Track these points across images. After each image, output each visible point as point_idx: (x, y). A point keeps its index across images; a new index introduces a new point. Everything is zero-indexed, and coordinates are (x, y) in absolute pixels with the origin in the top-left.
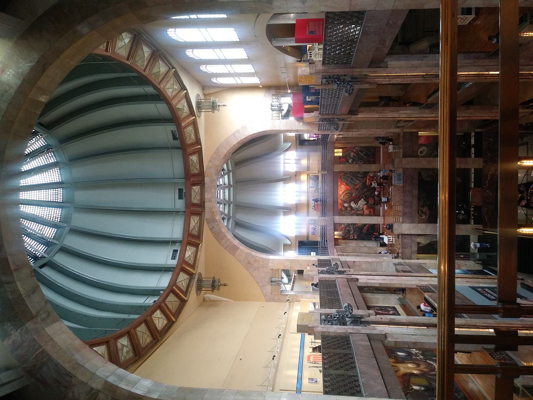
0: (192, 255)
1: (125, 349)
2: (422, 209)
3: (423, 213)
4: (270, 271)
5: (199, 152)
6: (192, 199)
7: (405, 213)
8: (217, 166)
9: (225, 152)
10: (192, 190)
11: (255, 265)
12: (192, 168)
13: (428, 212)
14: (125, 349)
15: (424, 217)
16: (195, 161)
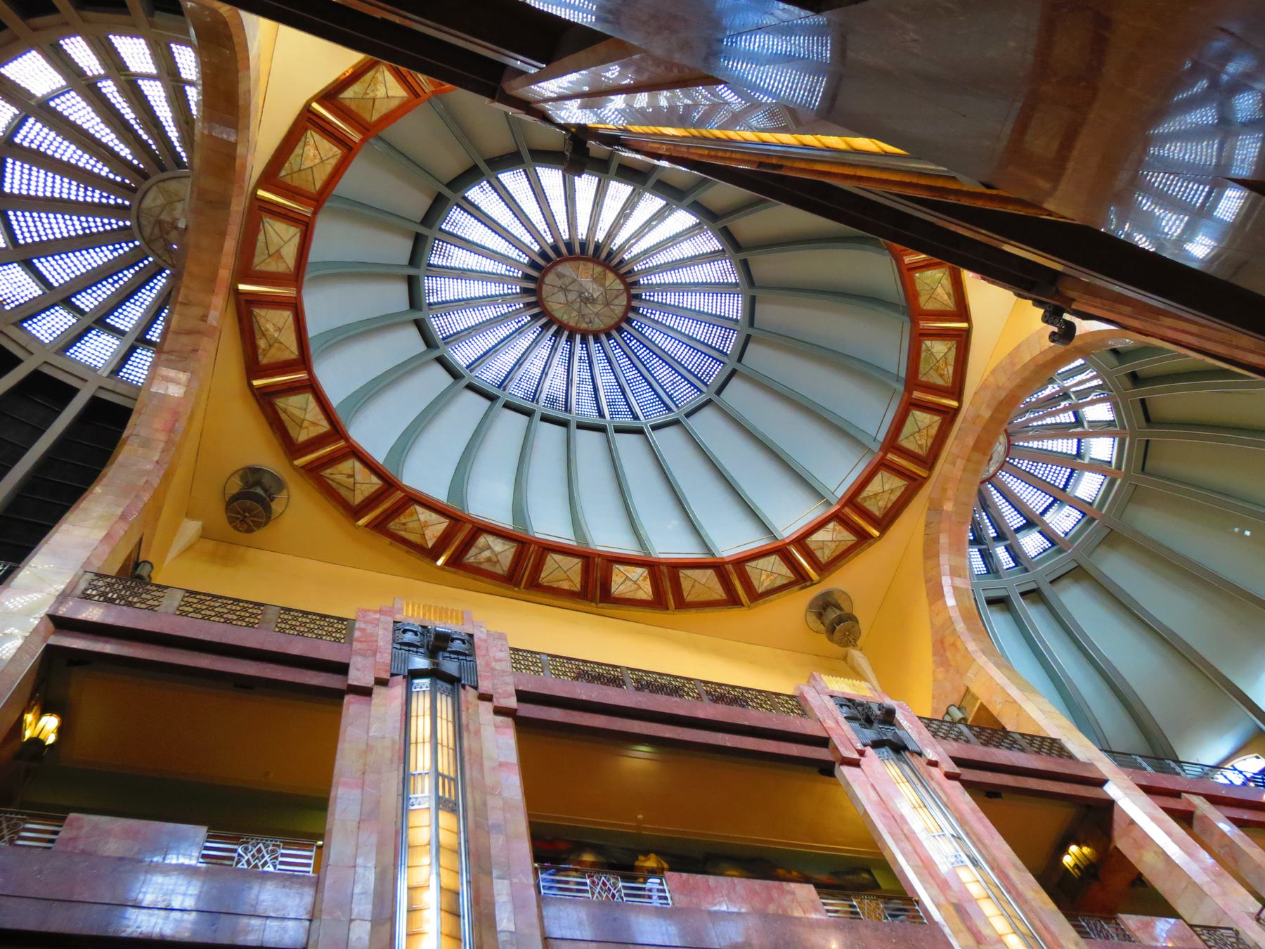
0: (833, 546)
1: (487, 554)
4: (963, 690)
5: (962, 340)
6: (902, 436)
8: (999, 388)
9: (1027, 358)
10: (910, 420)
11: (948, 654)
12: (923, 367)
16: (939, 356)
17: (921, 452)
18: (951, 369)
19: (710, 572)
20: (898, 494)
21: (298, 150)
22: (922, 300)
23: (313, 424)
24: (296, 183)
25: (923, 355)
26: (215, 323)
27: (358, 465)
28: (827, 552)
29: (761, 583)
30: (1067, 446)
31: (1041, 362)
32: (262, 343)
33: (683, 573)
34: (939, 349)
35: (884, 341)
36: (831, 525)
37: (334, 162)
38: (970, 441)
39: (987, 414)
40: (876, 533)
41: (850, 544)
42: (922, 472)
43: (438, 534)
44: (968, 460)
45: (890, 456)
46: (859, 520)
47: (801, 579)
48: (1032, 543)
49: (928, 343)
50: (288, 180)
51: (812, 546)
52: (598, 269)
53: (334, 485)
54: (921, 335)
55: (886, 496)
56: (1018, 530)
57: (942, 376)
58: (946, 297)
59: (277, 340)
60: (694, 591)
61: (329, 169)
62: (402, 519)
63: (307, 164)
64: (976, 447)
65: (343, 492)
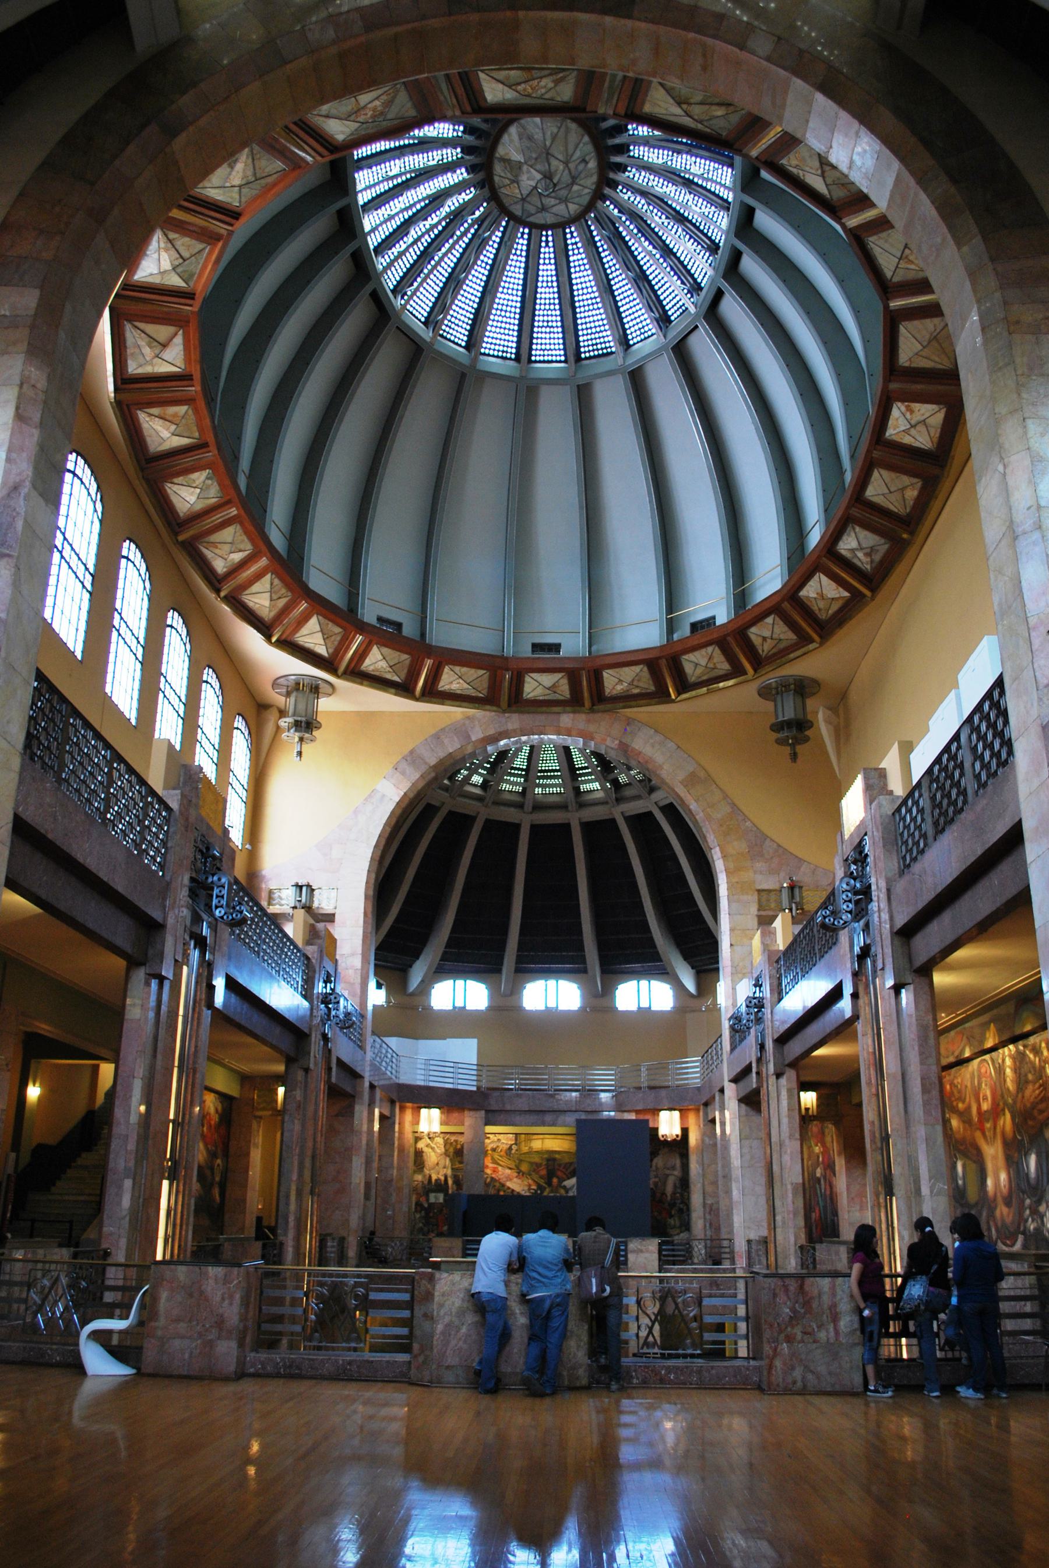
14: (860, 555)
21: (459, 692)
23: (710, 658)
24: (486, 685)
26: (617, 742)
27: (753, 630)
32: (636, 691)
37: (457, 669)
43: (834, 585)
50: (485, 692)
53: (774, 651)
59: (631, 683)
61: (464, 669)
62: (815, 608)
63: (466, 686)
65: (782, 646)
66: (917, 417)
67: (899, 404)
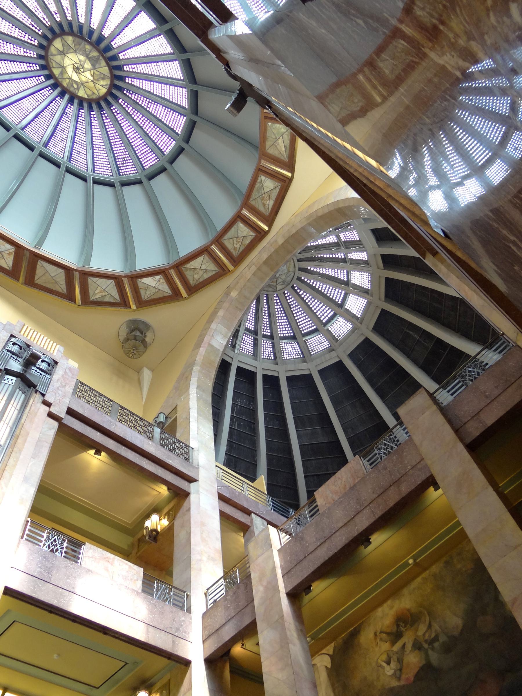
0: (154, 291)
2: (409, 646)
3: (400, 661)
5: (285, 184)
7: (302, 539)
10: (235, 226)
12: (254, 195)
13: (410, 674)
15: (389, 670)
16: (267, 190)
17: (235, 253)
18: (272, 203)
19: (61, 271)
20: (210, 274)
22: (268, 144)
25: (257, 185)
28: (148, 293)
29: (95, 294)
30: (337, 294)
31: (320, 214)
33: (40, 263)
34: (268, 184)
35: (241, 167)
36: (158, 277)
38: (265, 256)
39: (281, 241)
40: (184, 294)
41: (166, 295)
42: (231, 267)
44: (259, 269)
45: (213, 247)
46: (179, 281)
47: (124, 303)
48: (290, 350)
49: (263, 178)
51: (140, 285)
52: (95, 54)
54: (260, 169)
55: (201, 272)
56: (285, 338)
57: (264, 205)
58: (283, 149)
60: (43, 278)
64: (266, 262)
66: (5, 256)
67: (13, 250)
